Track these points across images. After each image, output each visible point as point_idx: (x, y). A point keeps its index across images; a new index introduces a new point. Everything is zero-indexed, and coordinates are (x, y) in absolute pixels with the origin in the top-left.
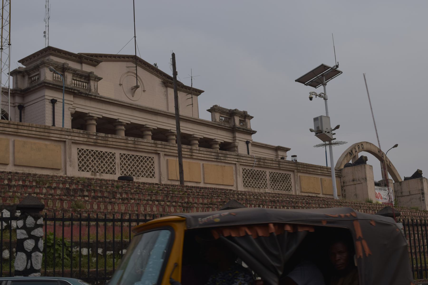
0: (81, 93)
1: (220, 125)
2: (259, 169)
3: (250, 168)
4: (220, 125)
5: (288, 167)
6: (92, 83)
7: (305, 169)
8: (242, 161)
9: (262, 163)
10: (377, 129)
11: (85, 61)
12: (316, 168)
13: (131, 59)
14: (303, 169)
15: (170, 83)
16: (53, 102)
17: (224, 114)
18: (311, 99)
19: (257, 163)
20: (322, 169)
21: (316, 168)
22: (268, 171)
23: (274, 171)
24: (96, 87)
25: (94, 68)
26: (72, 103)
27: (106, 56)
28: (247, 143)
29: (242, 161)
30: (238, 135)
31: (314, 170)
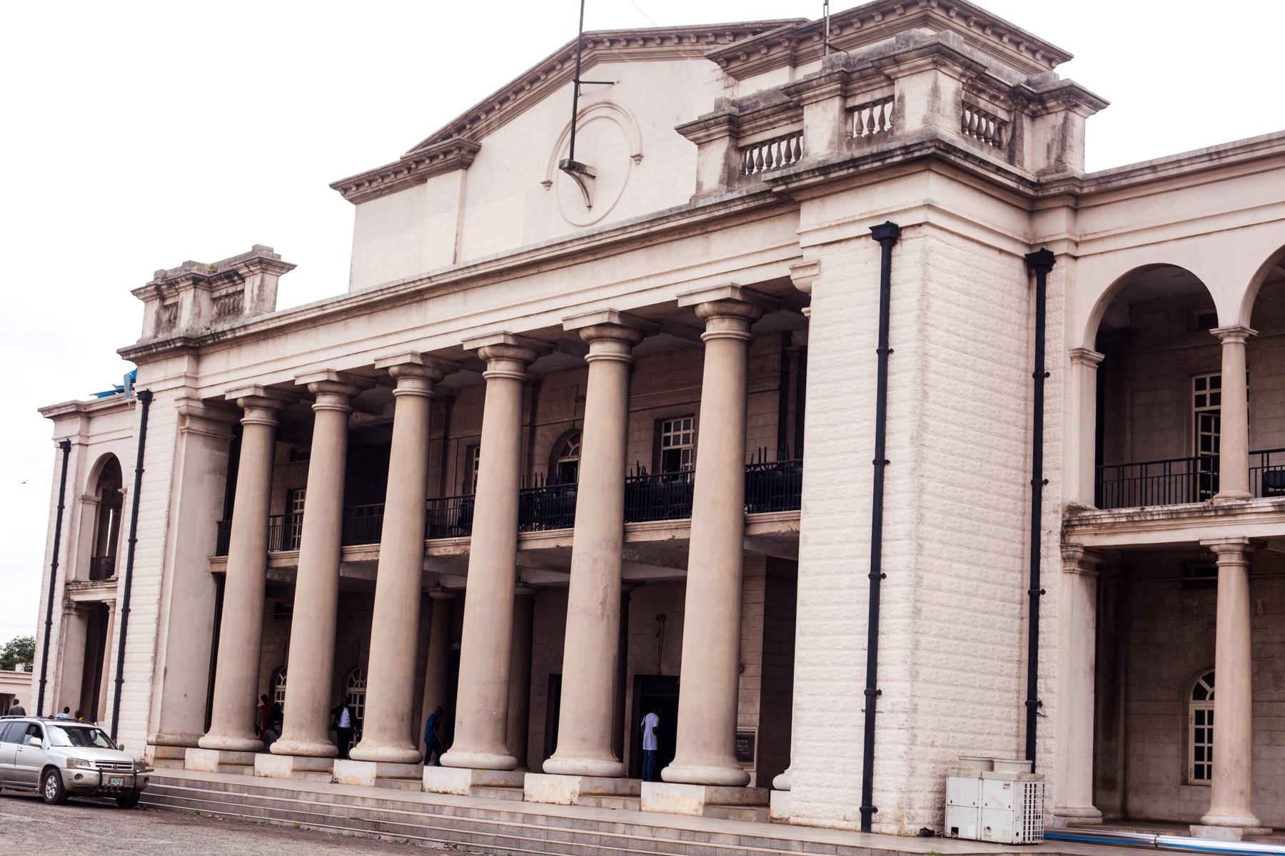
17: (771, 125)
25: (460, 172)
27: (486, 108)
28: (887, 236)
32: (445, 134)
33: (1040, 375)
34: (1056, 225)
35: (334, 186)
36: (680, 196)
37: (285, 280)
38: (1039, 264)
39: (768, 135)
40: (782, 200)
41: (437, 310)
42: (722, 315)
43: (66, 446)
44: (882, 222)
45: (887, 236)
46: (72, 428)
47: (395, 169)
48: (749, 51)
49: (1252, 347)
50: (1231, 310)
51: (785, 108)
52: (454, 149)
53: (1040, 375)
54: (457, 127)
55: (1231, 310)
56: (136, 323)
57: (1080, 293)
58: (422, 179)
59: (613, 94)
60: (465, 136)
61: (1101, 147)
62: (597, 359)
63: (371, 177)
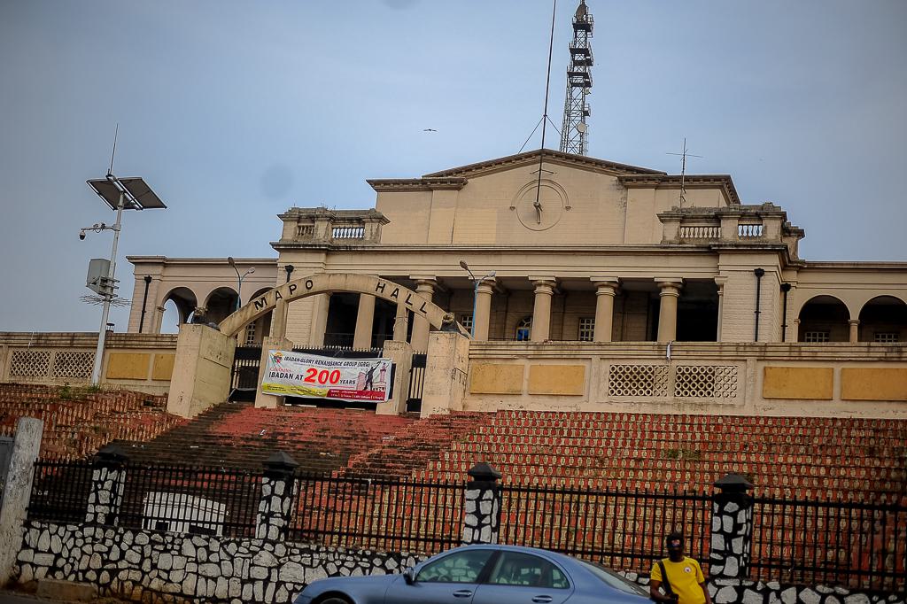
0: (339, 247)
1: (664, 248)
2: (39, 350)
3: (25, 350)
4: (664, 248)
5: (89, 342)
6: (368, 226)
7: (123, 342)
8: (13, 341)
9: (43, 342)
10: (223, 255)
11: (433, 185)
12: (147, 339)
13: (539, 158)
14: (117, 342)
15: (627, 180)
16: (290, 269)
18: (82, 237)
19: (35, 341)
20: (159, 339)
21: (147, 339)
22: (53, 352)
23: (64, 351)
24: (374, 231)
26: (321, 265)
27: (478, 167)
28: (759, 273)
29: (13, 341)
30: (723, 260)
31: (141, 343)
32: (449, 173)
33: (784, 326)
34: (792, 277)
35: (369, 181)
36: (657, 240)
37: (384, 227)
38: (785, 288)
39: (696, 225)
40: (712, 251)
41: (506, 260)
42: (673, 287)
43: (148, 280)
44: (757, 268)
45: (759, 273)
46: (154, 271)
47: (415, 182)
48: (642, 179)
49: (860, 327)
50: (854, 315)
51: (707, 218)
52: (453, 180)
53: (784, 326)
54: (458, 171)
55: (854, 315)
56: (278, 231)
57: (798, 299)
58: (431, 190)
59: (552, 178)
60: (459, 177)
61: (805, 251)
62: (605, 294)
63: (386, 182)
